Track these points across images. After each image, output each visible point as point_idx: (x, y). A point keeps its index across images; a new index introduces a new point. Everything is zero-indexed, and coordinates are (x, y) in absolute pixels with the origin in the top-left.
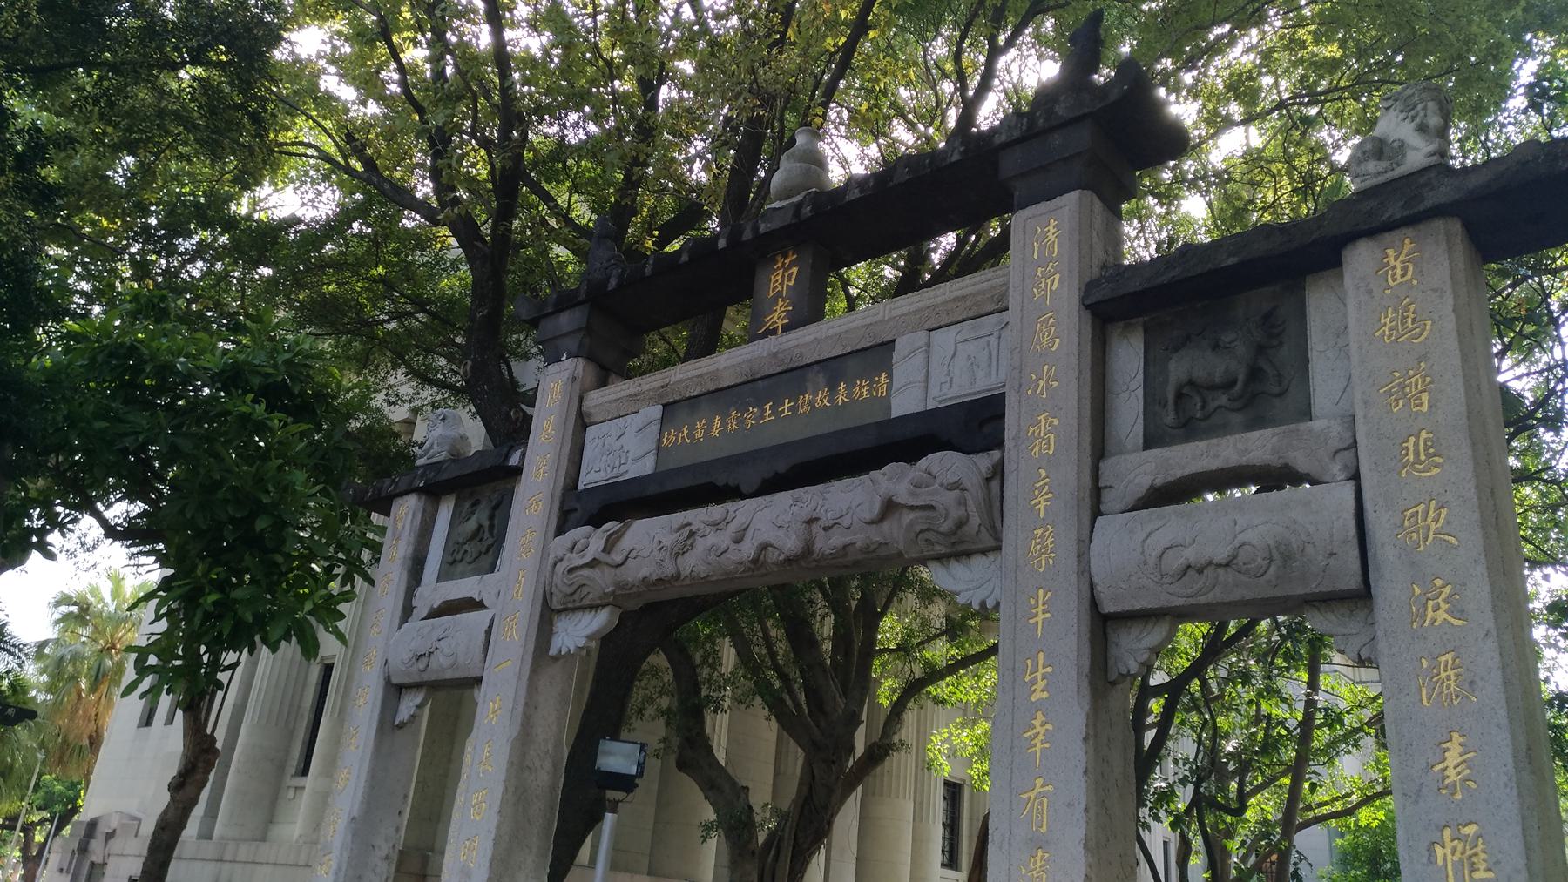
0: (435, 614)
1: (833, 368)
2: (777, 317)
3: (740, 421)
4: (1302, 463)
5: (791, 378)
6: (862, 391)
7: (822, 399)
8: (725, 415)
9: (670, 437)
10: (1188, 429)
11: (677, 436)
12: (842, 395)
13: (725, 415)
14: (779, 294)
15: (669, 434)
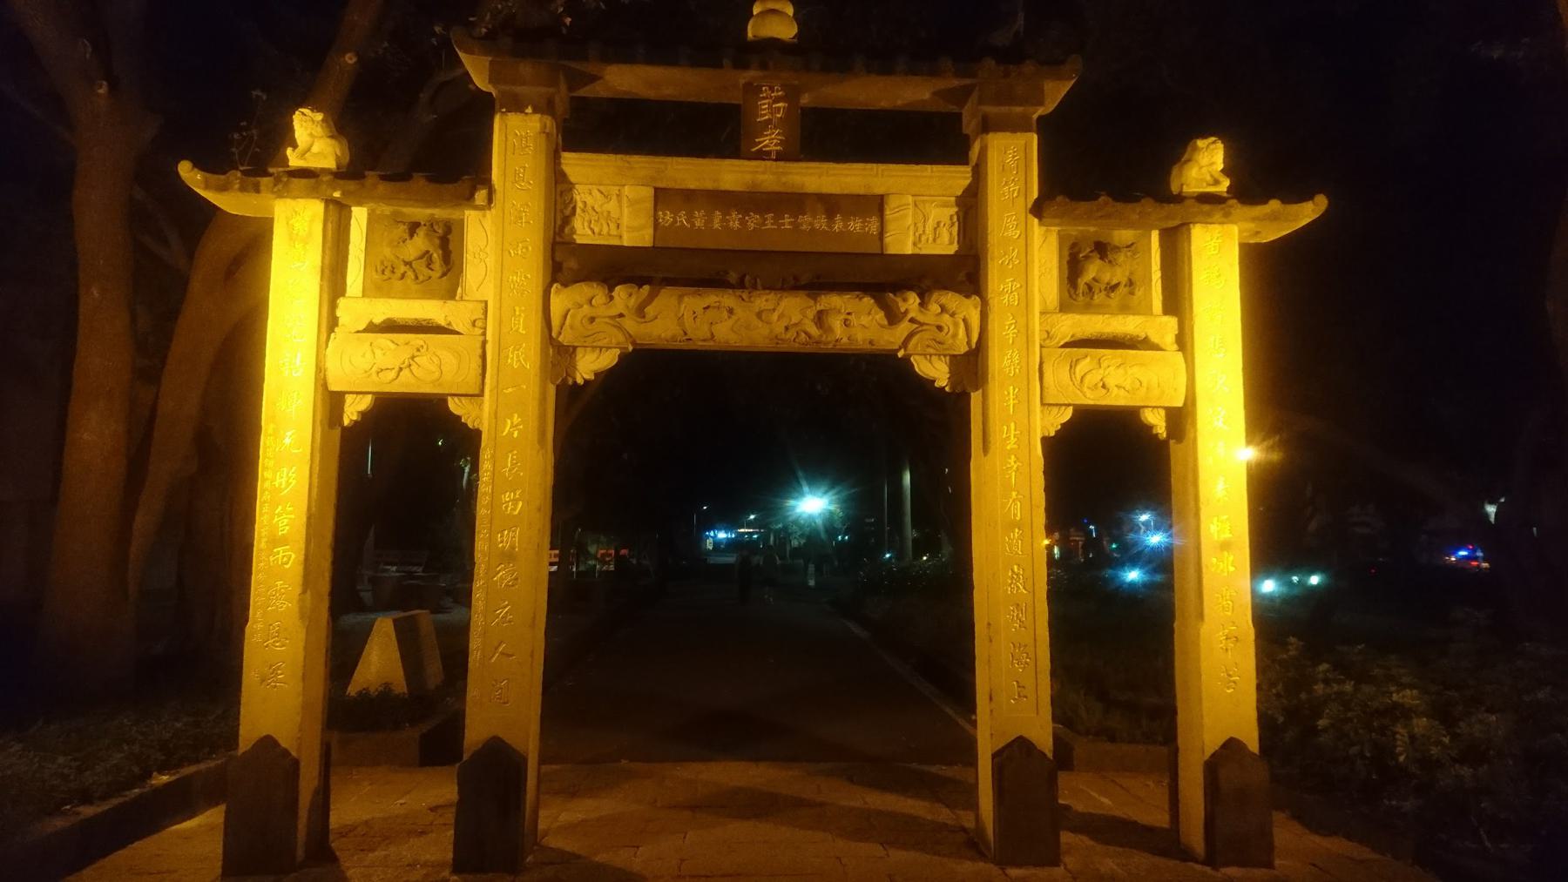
0: (372, 328)
1: (832, 204)
2: (770, 140)
3: (743, 222)
4: (1155, 339)
5: (795, 202)
6: (855, 225)
7: (821, 223)
8: (726, 213)
9: (667, 217)
10: (1088, 308)
11: (674, 218)
12: (838, 225)
13: (726, 213)
14: (769, 122)
15: (665, 215)
